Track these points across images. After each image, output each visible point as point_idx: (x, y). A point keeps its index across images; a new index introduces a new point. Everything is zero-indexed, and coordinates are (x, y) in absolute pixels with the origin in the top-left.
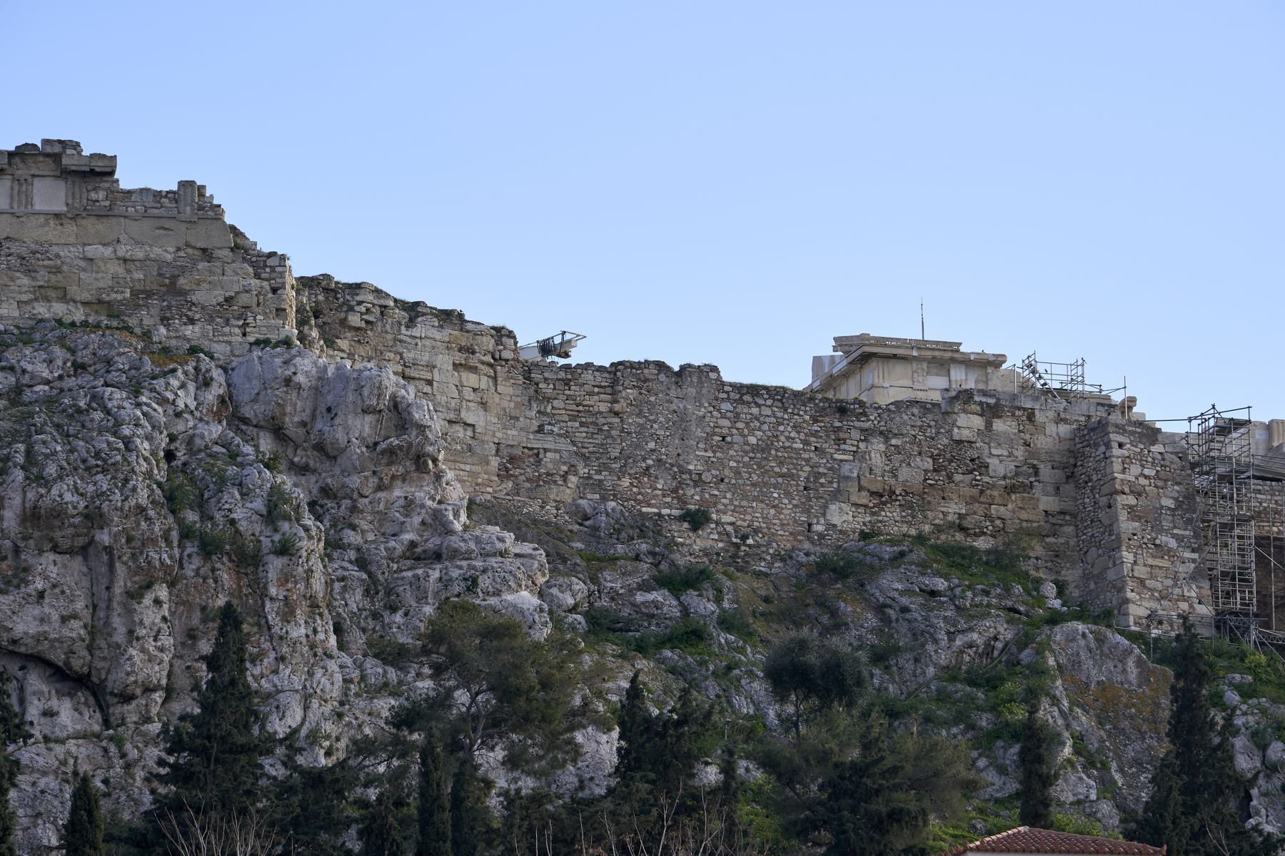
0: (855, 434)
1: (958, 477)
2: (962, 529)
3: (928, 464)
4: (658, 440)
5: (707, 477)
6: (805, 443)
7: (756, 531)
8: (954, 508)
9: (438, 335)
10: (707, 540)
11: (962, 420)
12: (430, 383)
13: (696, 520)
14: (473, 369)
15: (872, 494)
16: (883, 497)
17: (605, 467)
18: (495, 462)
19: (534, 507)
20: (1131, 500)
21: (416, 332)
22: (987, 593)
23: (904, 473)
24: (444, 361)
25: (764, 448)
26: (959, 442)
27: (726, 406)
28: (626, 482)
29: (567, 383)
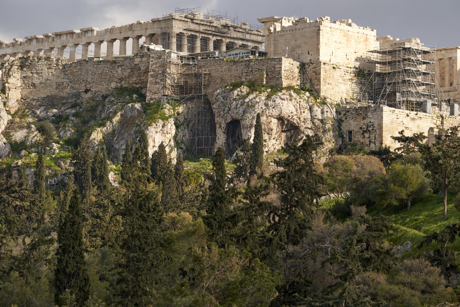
0: (116, 67)
1: (135, 72)
2: (136, 83)
3: (130, 70)
4: (83, 76)
5: (91, 82)
6: (109, 71)
7: (99, 91)
8: (134, 79)
9: (43, 63)
10: (89, 95)
11: (136, 60)
12: (42, 73)
13: (87, 91)
14: (51, 68)
15: (119, 79)
16: (121, 80)
17: (74, 83)
18: (55, 87)
19: (62, 94)
20: (152, 73)
21: (39, 63)
22: (120, 100)
23: (125, 73)
24: (45, 68)
25: (101, 74)
26: (136, 65)
27: (96, 66)
28: (77, 86)
29: (70, 67)
